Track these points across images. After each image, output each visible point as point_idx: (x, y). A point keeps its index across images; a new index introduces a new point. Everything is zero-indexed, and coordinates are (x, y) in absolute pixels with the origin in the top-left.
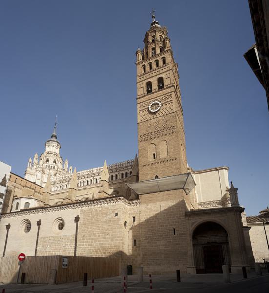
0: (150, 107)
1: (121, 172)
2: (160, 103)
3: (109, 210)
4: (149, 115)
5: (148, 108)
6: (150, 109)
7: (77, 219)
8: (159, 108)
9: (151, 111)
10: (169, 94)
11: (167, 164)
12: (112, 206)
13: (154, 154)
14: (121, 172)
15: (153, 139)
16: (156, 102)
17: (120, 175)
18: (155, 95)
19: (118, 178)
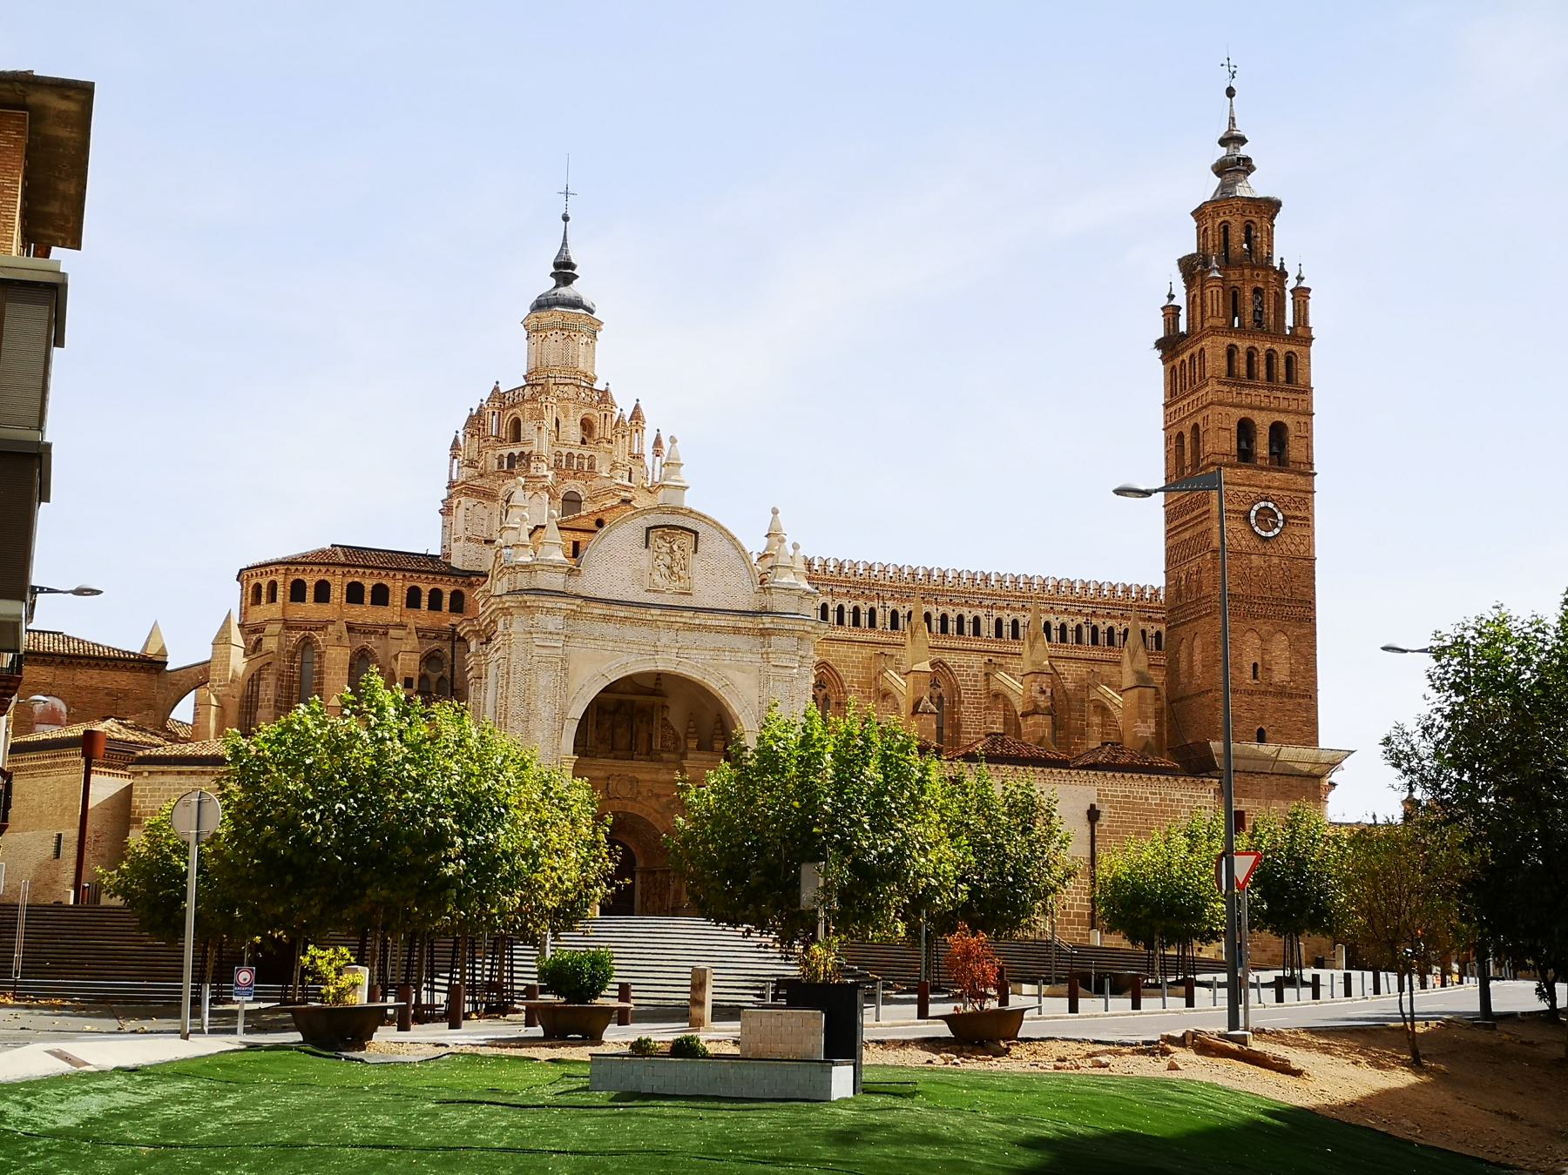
0: (1253, 514)
1: (996, 614)
2: (1280, 516)
3: (1183, 807)
4: (1248, 537)
5: (1247, 518)
6: (1253, 521)
7: (1093, 815)
8: (1277, 531)
9: (1257, 529)
10: (1301, 495)
11: (1289, 704)
12: (1190, 796)
13: (1255, 665)
14: (996, 614)
15: (1255, 617)
16: (1271, 505)
17: (993, 621)
18: (1264, 477)
19: (984, 633)
